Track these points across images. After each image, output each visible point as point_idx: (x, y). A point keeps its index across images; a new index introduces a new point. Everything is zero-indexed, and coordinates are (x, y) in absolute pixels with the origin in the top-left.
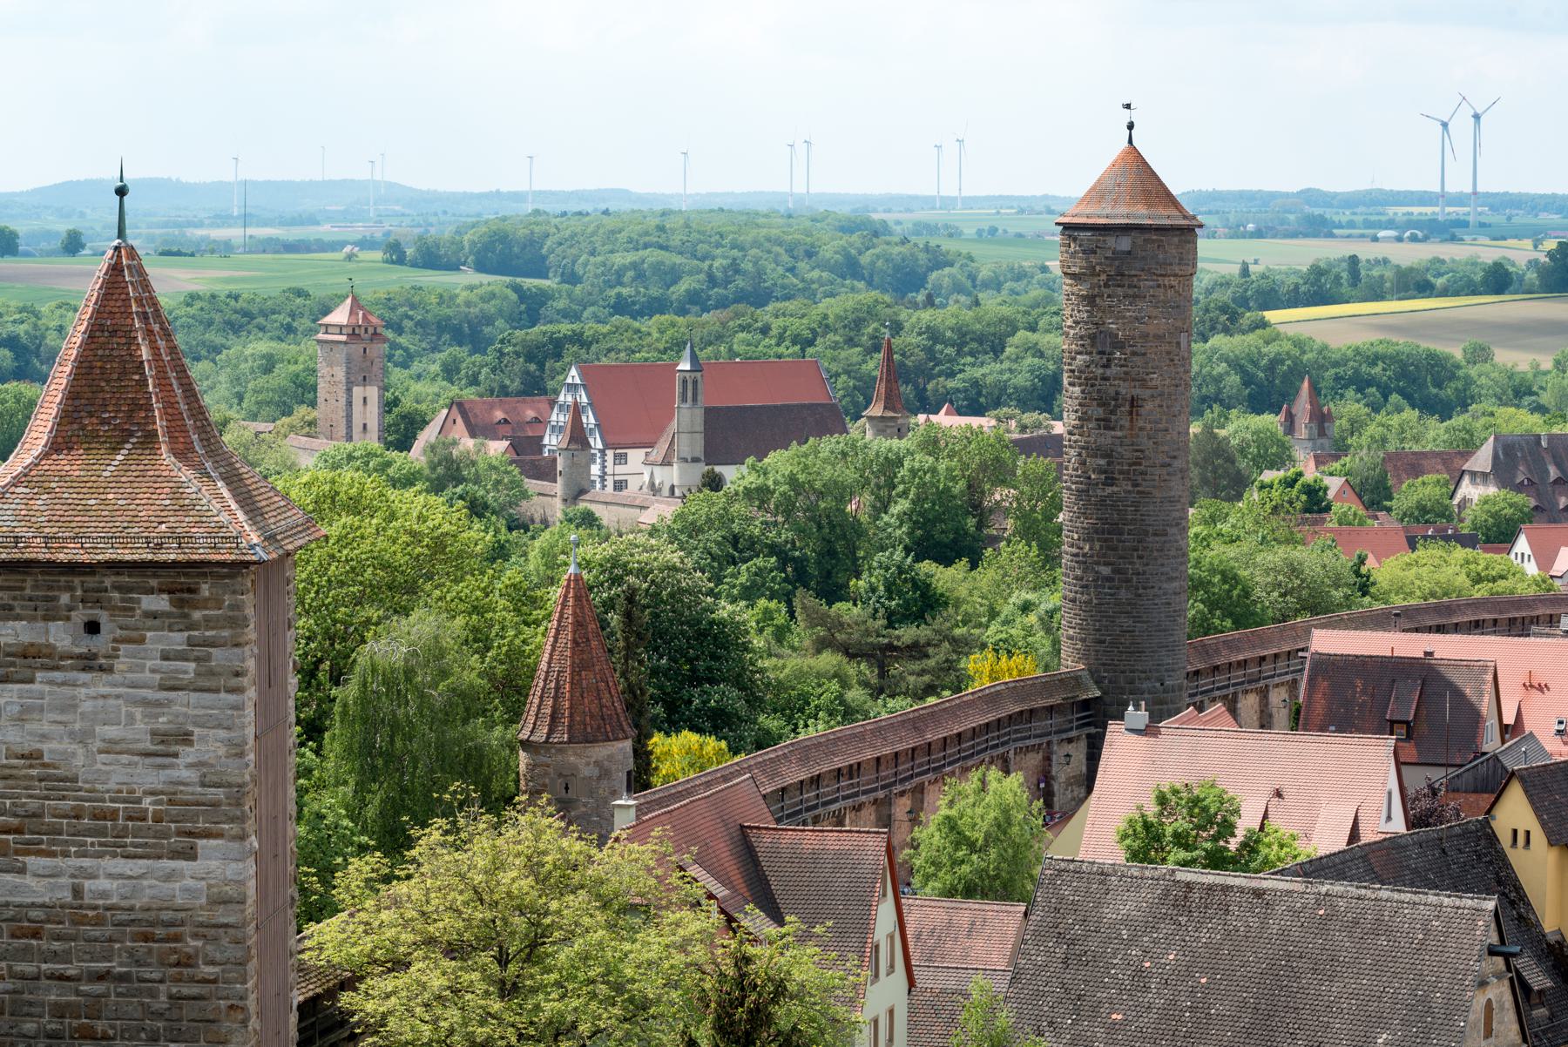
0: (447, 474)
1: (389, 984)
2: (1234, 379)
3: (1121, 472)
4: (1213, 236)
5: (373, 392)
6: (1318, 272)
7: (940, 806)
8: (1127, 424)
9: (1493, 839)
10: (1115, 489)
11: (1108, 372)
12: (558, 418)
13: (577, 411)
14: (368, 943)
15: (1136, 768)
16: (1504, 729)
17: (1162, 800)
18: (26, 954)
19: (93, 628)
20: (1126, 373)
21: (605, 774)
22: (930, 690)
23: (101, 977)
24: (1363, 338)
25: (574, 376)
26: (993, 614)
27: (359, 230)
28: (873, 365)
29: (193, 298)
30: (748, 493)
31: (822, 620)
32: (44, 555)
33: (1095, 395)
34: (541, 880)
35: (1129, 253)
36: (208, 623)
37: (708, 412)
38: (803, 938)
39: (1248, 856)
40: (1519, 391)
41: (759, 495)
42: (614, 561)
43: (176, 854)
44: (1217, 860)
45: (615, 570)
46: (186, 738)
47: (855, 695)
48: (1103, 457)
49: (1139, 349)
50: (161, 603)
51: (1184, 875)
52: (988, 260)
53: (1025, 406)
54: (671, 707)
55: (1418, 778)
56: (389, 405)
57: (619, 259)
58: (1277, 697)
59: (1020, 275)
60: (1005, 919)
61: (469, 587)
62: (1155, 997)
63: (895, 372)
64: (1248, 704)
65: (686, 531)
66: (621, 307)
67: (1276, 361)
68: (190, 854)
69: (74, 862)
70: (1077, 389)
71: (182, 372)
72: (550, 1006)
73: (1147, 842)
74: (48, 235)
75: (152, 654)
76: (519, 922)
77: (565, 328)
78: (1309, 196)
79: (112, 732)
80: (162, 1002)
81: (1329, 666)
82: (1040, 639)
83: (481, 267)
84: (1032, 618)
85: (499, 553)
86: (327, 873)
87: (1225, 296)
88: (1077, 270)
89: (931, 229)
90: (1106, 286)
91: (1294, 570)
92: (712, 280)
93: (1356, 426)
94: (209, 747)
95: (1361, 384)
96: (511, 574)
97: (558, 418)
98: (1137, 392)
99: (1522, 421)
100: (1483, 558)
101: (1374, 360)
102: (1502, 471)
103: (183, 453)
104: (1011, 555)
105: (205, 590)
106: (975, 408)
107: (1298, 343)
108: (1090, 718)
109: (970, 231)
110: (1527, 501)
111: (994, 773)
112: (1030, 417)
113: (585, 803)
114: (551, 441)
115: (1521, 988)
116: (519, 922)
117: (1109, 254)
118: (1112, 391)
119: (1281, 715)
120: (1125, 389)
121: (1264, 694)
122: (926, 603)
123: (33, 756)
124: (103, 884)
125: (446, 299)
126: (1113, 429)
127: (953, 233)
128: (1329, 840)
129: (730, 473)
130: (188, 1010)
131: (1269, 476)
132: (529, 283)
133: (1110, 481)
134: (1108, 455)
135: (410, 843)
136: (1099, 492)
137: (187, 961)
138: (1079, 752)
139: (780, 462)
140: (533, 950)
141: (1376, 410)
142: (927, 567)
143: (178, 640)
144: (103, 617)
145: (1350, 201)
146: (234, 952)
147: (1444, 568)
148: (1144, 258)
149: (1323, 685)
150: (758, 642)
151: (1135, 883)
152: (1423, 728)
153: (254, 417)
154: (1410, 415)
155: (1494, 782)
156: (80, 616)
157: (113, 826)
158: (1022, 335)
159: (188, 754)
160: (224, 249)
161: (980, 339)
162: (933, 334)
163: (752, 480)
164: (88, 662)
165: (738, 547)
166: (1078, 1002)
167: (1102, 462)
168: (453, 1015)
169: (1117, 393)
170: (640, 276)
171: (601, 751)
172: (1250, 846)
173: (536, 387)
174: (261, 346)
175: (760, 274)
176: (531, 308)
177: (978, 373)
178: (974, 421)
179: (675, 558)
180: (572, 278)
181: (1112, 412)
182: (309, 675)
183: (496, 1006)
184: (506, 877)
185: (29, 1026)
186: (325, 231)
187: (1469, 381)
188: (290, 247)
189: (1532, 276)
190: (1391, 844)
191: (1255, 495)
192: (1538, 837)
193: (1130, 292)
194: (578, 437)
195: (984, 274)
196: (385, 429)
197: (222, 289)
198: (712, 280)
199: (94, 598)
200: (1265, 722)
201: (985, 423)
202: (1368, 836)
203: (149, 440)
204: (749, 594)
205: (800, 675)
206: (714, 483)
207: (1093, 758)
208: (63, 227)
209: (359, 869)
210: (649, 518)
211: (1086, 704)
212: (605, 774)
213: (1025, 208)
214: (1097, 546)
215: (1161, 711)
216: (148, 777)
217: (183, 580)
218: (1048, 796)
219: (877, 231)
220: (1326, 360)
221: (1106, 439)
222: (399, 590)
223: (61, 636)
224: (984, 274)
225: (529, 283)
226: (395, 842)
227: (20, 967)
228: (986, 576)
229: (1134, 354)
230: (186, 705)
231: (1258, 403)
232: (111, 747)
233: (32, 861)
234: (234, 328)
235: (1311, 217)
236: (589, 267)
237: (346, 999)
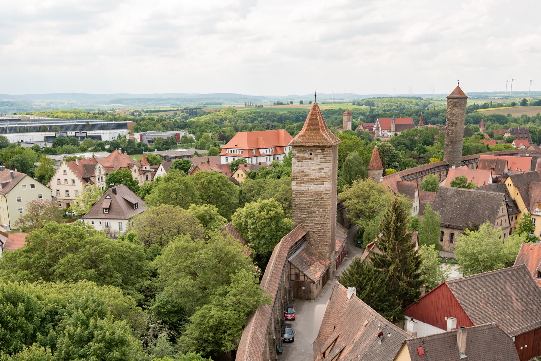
0: (359, 134)
1: (349, 201)
2: (472, 120)
4: (470, 99)
5: (350, 123)
6: (485, 104)
7: (425, 179)
9: (505, 185)
12: (375, 126)
13: (378, 125)
14: (346, 196)
15: (454, 173)
16: (508, 169)
17: (456, 179)
18: (301, 197)
19: (311, 154)
21: (379, 174)
22: (425, 163)
23: (311, 200)
24: (491, 114)
25: (377, 120)
26: (434, 152)
27: (349, 100)
28: (420, 119)
29: (327, 110)
30: (401, 136)
31: (410, 153)
32: (305, 145)
34: (370, 188)
36: (326, 154)
37: (396, 125)
38: (406, 197)
39: (469, 187)
40: (516, 121)
41: (402, 136)
42: (382, 145)
43: (321, 184)
44: (464, 187)
45: (382, 146)
46: (323, 169)
47: (415, 164)
50: (320, 151)
51: (459, 189)
52: (437, 103)
53: (441, 124)
54: (389, 165)
55: (494, 176)
56: (352, 124)
57: (385, 104)
58: (475, 165)
59: (441, 105)
60: (433, 194)
61: (361, 148)
62: (454, 205)
63: (423, 119)
64: (470, 166)
65: (392, 141)
66: (385, 110)
67: (477, 117)
68: (323, 184)
69: (308, 185)
71: (323, 120)
72: (370, 205)
73: (454, 184)
74: (307, 101)
75: (318, 157)
76: (366, 194)
77: (377, 113)
78: (485, 93)
79: (313, 168)
80: (319, 203)
81: (484, 161)
82: (441, 156)
83: (366, 105)
84: (440, 153)
85: (367, 144)
86: (341, 187)
87: (471, 108)
89: (429, 99)
91: (478, 146)
92: (397, 107)
93: (489, 126)
94: (326, 170)
95: (491, 120)
96: (367, 147)
97: (375, 126)
99: (514, 125)
100: (508, 144)
101: (493, 116)
102: (512, 132)
103: (323, 131)
104: (437, 144)
105: (326, 149)
106: (434, 124)
107: (482, 115)
108: (447, 167)
109: (434, 99)
110: (515, 136)
111: (433, 174)
112: (441, 125)
113: (376, 178)
114: (374, 129)
115: (508, 206)
116: (366, 194)
119: (475, 167)
121: (472, 164)
122: (425, 151)
123: (303, 171)
124: (312, 188)
125: (360, 110)
127: (432, 99)
128: (480, 185)
129: (398, 133)
130: (322, 204)
131: (476, 133)
132: (372, 107)
134: (452, 130)
135: (352, 183)
137: (323, 198)
138: (445, 172)
139: (405, 131)
140: (368, 197)
141: (492, 123)
142: (425, 146)
143: (322, 156)
144: (312, 153)
145: (491, 93)
146: (329, 197)
147: (501, 145)
149: (481, 163)
150: (401, 156)
151: (452, 190)
152: (496, 169)
153: (334, 126)
154: (498, 124)
155: (506, 177)
156: (309, 153)
157: (313, 180)
158: (441, 114)
159: (323, 171)
160: (331, 103)
161: (435, 114)
162: (428, 113)
163: (402, 134)
164: (310, 159)
165: (399, 144)
166: (442, 205)
168: (357, 206)
170: (387, 106)
171: (379, 171)
172: (469, 185)
173: (373, 122)
174: (335, 116)
175: (404, 106)
176: (373, 110)
177: (434, 119)
178: (433, 126)
179: (390, 145)
180: (378, 107)
182: (340, 161)
183: (363, 205)
184: (365, 188)
185: (302, 206)
186: (344, 101)
187: (507, 119)
188: (340, 103)
189: (519, 104)
190: (490, 185)
191: (473, 136)
192: (512, 185)
194: (378, 129)
195: (436, 105)
196: (352, 128)
197: (330, 109)
198: (397, 107)
199: (311, 150)
200: (473, 168)
201: (435, 126)
202: (486, 184)
203: (319, 129)
204: (400, 150)
205: (408, 161)
206: (396, 135)
207: (447, 173)
208: (309, 100)
209: (346, 186)
210: (387, 140)
211: (447, 165)
212: (379, 174)
213: (442, 95)
215: (457, 166)
216: (318, 174)
217: (323, 148)
218: (440, 178)
219: (421, 99)
220: (485, 117)
221: (452, 128)
222: (351, 149)
223: (307, 155)
224: (436, 105)
225: (372, 107)
226: (351, 184)
227: (302, 199)
228: (434, 147)
230: (323, 165)
231: (475, 123)
232: (313, 170)
233: (303, 185)
234: (332, 114)
235: (484, 96)
236: (380, 105)
237: (343, 203)
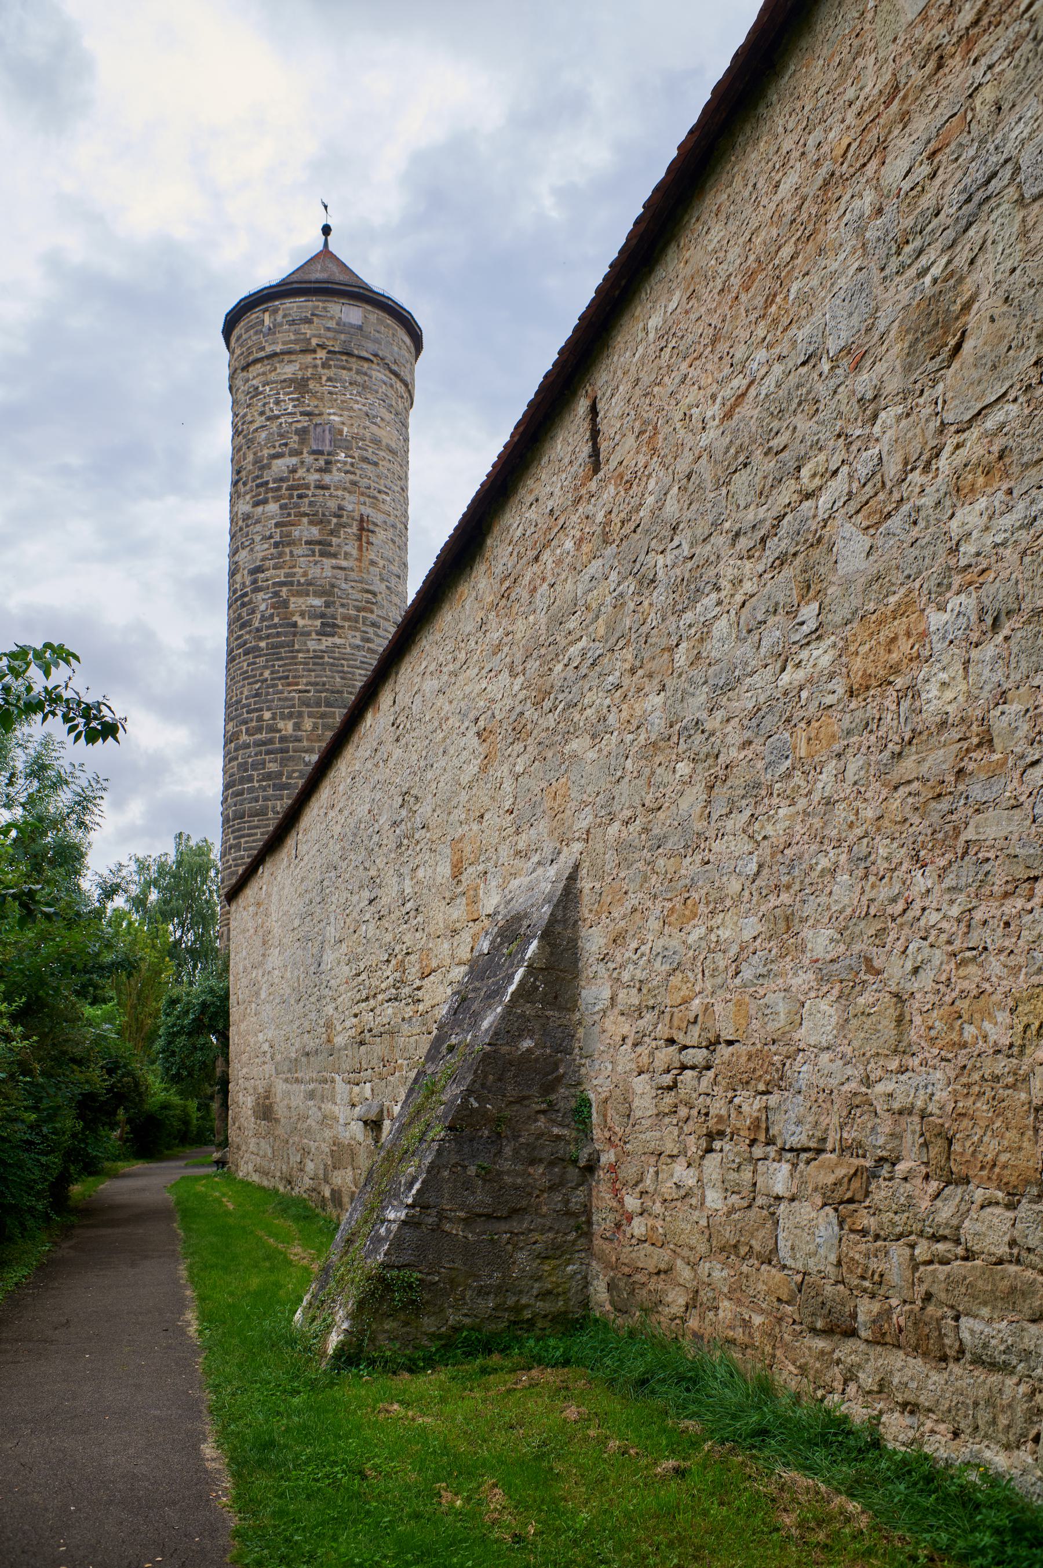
3: (346, 618)
8: (355, 552)
10: (337, 640)
11: (327, 479)
20: (354, 483)
33: (305, 509)
35: (360, 328)
48: (318, 594)
49: (369, 455)
70: (273, 507)
88: (278, 348)
90: (325, 365)
98: (367, 510)
117: (332, 324)
118: (332, 504)
120: (350, 502)
126: (335, 556)
133: (329, 628)
136: (312, 645)
148: (377, 341)
167: (318, 602)
169: (341, 508)
181: (332, 533)
193: (359, 379)
214: (308, 724)
229: (365, 460)
